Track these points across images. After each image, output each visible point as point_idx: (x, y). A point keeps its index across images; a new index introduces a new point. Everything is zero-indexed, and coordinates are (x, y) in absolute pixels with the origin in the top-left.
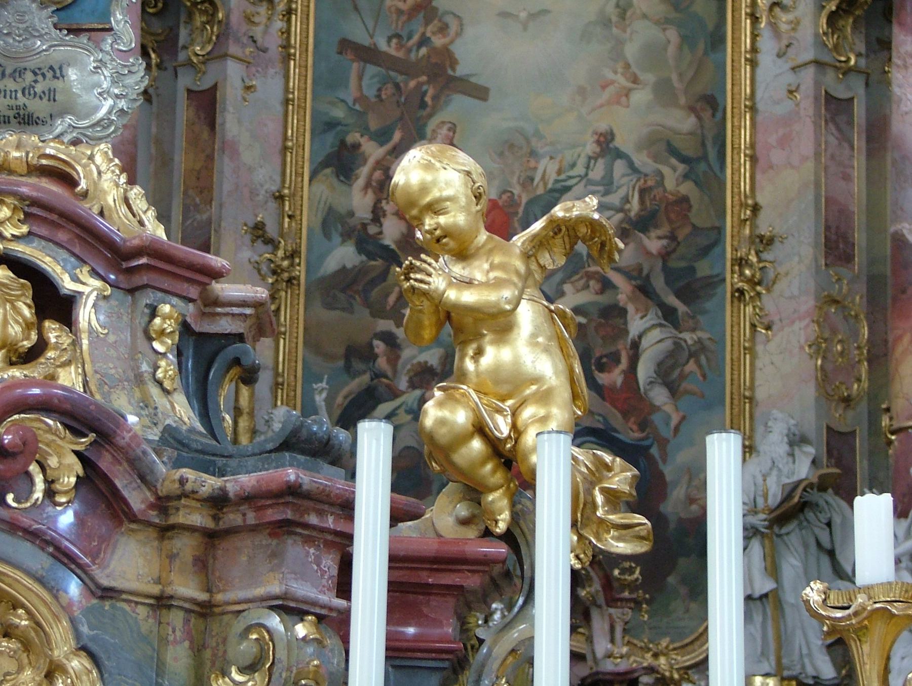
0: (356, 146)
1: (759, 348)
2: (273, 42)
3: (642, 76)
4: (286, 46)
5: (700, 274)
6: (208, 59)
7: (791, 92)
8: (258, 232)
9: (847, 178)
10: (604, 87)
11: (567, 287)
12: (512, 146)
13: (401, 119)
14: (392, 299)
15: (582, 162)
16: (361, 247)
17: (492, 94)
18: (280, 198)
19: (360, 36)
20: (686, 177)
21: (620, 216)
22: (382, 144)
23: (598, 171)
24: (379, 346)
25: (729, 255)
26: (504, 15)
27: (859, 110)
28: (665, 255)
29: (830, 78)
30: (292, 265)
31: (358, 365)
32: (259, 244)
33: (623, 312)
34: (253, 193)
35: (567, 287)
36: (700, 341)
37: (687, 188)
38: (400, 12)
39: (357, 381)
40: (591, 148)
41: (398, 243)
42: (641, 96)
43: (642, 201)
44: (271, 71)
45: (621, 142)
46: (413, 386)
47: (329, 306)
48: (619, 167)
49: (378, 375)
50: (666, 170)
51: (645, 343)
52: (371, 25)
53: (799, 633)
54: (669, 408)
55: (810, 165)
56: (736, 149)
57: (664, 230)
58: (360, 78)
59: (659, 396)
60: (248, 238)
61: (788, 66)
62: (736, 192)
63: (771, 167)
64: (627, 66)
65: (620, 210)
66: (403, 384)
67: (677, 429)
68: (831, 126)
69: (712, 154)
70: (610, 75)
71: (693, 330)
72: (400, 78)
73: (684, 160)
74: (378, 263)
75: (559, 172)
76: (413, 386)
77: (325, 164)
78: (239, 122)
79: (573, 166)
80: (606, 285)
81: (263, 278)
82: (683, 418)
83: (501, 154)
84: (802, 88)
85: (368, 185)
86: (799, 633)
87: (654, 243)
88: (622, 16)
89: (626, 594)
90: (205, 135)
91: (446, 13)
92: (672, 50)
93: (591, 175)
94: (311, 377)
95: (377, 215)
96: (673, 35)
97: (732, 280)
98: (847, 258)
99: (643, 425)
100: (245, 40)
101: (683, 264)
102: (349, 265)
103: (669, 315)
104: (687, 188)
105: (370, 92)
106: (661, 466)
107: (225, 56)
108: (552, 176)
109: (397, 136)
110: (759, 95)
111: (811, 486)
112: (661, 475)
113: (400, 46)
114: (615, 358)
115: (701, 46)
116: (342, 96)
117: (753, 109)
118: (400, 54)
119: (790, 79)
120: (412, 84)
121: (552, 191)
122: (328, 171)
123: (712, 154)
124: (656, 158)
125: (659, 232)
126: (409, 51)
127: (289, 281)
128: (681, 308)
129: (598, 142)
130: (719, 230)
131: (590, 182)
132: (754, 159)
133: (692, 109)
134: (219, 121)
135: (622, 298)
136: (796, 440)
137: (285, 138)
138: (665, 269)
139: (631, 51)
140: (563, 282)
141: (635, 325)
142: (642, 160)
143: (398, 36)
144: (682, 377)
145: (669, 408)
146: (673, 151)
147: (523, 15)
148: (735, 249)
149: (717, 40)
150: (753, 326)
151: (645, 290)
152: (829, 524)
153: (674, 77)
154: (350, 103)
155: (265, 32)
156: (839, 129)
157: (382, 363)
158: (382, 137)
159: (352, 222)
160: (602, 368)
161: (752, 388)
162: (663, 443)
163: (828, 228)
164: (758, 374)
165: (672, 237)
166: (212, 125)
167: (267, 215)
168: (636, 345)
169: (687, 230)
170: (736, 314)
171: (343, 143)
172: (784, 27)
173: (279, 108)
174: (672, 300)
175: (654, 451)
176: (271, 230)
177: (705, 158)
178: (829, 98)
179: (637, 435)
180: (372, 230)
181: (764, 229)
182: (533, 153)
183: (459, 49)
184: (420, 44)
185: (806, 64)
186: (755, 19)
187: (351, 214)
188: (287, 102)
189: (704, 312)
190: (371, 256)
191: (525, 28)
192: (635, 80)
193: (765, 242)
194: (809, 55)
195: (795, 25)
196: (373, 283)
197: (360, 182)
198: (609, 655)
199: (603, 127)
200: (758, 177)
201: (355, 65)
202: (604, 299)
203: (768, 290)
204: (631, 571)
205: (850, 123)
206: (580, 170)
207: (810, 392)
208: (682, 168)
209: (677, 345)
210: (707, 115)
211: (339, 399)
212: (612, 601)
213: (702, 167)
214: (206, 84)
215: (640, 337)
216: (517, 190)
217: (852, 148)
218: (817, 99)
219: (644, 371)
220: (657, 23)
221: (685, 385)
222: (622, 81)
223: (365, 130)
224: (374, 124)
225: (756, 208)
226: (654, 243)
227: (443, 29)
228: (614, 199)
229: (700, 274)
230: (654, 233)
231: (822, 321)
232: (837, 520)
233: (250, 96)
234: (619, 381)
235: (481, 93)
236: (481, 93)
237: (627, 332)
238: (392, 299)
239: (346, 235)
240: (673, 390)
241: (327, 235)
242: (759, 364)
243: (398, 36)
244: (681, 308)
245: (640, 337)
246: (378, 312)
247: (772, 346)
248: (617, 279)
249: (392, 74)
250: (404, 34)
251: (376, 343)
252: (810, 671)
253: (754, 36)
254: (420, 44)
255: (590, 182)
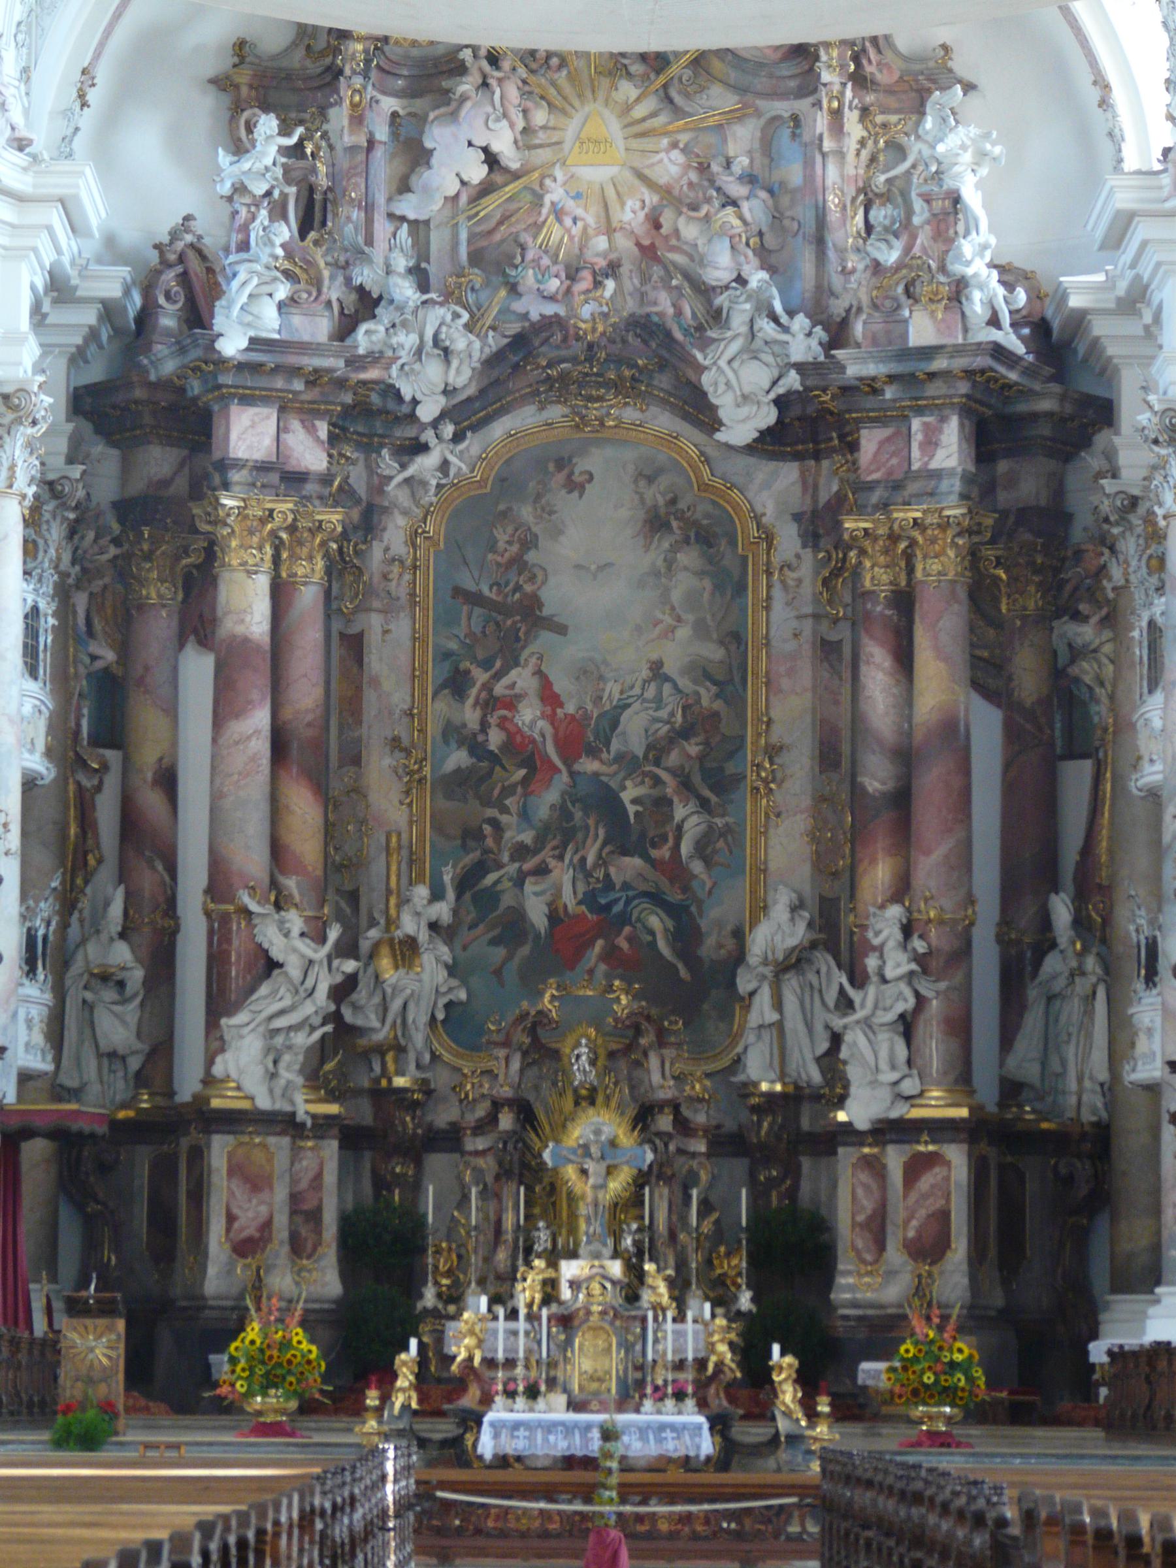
0: (468, 672)
1: (771, 831)
2: (402, 592)
3: (684, 616)
4: (413, 595)
5: (728, 772)
6: (357, 610)
7: (796, 635)
8: (395, 743)
9: (837, 703)
10: (655, 625)
11: (628, 783)
12: (585, 672)
13: (501, 650)
14: (496, 792)
15: (639, 684)
16: (472, 752)
17: (571, 634)
18: (412, 716)
19: (470, 586)
20: (717, 696)
21: (667, 727)
22: (487, 670)
23: (651, 692)
24: (487, 829)
25: (749, 757)
26: (578, 567)
27: (847, 650)
28: (701, 758)
29: (824, 626)
30: (421, 768)
31: (471, 843)
32: (397, 754)
33: (670, 803)
34: (391, 713)
35: (628, 783)
36: (727, 824)
37: (718, 705)
38: (498, 564)
39: (471, 856)
40: (645, 673)
41: (500, 749)
42: (683, 633)
43: (684, 715)
44: (402, 615)
45: (670, 668)
46: (513, 859)
47: (449, 796)
48: (667, 688)
49: (486, 851)
50: (702, 691)
51: (686, 826)
52: (476, 574)
53: (796, 1049)
54: (704, 876)
55: (809, 695)
56: (755, 675)
57: (699, 739)
58: (469, 619)
59: (697, 867)
60: (387, 749)
61: (794, 613)
62: (755, 709)
63: (781, 691)
64: (673, 608)
65: (668, 722)
66: (506, 857)
67: (710, 893)
68: (825, 664)
69: (737, 679)
70: (660, 616)
71: (723, 816)
72: (500, 618)
73: (715, 683)
74: (485, 764)
75: (622, 692)
76: (513, 859)
77: (443, 686)
78: (381, 659)
79: (632, 687)
80: (657, 781)
81: (400, 778)
82: (715, 884)
83: (578, 678)
84: (804, 634)
85: (476, 703)
86: (796, 1049)
87: (693, 749)
88: (669, 568)
89: (672, 1039)
90: (355, 670)
91: (534, 565)
92: (706, 595)
93: (646, 695)
94: (440, 857)
95: (484, 726)
96: (707, 583)
97: (751, 776)
98: (836, 765)
99: (685, 889)
100: (383, 595)
101: (715, 765)
102: (463, 766)
103: (704, 804)
104: (718, 705)
105: (477, 630)
106: (699, 920)
107: (369, 610)
108: (616, 696)
109: (498, 664)
110: (772, 632)
111: (805, 948)
112: (698, 927)
113: (499, 592)
114: (664, 838)
115: (729, 593)
116: (455, 632)
117: (767, 645)
118: (499, 599)
119: (795, 624)
120: (509, 622)
121: (616, 707)
122: (446, 691)
123: (737, 679)
124: (695, 682)
125: (699, 739)
126: (506, 596)
127: (420, 781)
128: (714, 799)
129: (651, 669)
130: (743, 738)
131: (645, 701)
132: (768, 684)
133: (721, 643)
134: (366, 660)
135: (669, 791)
136: (794, 909)
137: (414, 669)
138: (702, 769)
139: (676, 596)
140: (625, 779)
141: (680, 812)
142: (684, 683)
143: (498, 584)
144: (715, 852)
145: (704, 876)
146: (707, 676)
147: (593, 567)
148: (754, 756)
149: (741, 588)
150: (766, 814)
151: (686, 785)
152: (818, 972)
153: (709, 617)
154: (462, 636)
155: (399, 585)
156: (832, 666)
157: (489, 842)
158: (486, 665)
159: (464, 732)
160: (654, 845)
161: (766, 863)
162: (700, 903)
163: (822, 743)
164: (770, 851)
165: (706, 743)
166: (359, 660)
167: (401, 730)
168: (679, 828)
169: (718, 738)
170: (755, 802)
171: (457, 670)
172: (791, 583)
173: (409, 643)
174: (707, 793)
175: (693, 909)
176: (406, 742)
177: (731, 681)
178: (824, 642)
179: (680, 897)
180: (480, 738)
181: (774, 739)
182: (601, 678)
183: (545, 595)
184: (515, 591)
185: (806, 616)
186: (769, 574)
187: (464, 725)
188: (415, 639)
189: (732, 802)
190: (480, 760)
191: (595, 577)
192: (679, 619)
193: (773, 751)
194: (808, 609)
195: (799, 581)
196: (481, 780)
197: (470, 701)
198: (662, 1087)
199: (654, 656)
200: (772, 698)
201: (465, 608)
202: (655, 792)
203: (779, 786)
204: (676, 1023)
205: (840, 660)
206: (637, 691)
207: (806, 869)
208: (714, 689)
209: (711, 828)
210: (733, 647)
211: (458, 870)
212: (661, 1043)
213: (730, 688)
214: (353, 630)
215: (683, 821)
216: (589, 707)
217: (841, 679)
218: (814, 643)
219: (686, 848)
220: (696, 573)
221: (716, 858)
222: (669, 620)
223: (474, 659)
224: (481, 654)
225: (769, 723)
226: (693, 749)
227: (532, 579)
228: (663, 714)
229: (728, 772)
230: (693, 741)
231: (816, 813)
232: (824, 970)
233: (388, 637)
234: (667, 855)
235: (562, 630)
236: (562, 630)
237: (672, 818)
238: (496, 792)
239: (461, 744)
240: (708, 862)
241: (446, 742)
242: (771, 843)
243: (498, 584)
244: (714, 799)
245: (683, 821)
246: (487, 802)
247: (781, 830)
248: (664, 775)
249: (494, 614)
250: (502, 582)
251: (485, 826)
252: (804, 1076)
253: (769, 587)
254: (515, 591)
255: (645, 701)
